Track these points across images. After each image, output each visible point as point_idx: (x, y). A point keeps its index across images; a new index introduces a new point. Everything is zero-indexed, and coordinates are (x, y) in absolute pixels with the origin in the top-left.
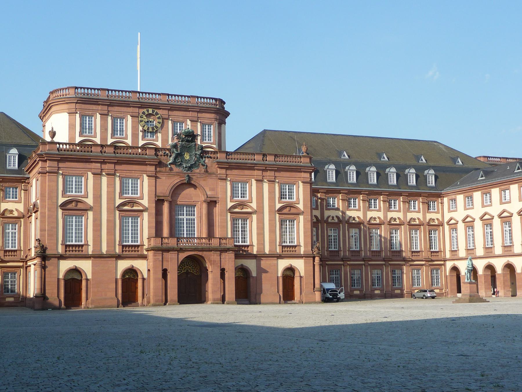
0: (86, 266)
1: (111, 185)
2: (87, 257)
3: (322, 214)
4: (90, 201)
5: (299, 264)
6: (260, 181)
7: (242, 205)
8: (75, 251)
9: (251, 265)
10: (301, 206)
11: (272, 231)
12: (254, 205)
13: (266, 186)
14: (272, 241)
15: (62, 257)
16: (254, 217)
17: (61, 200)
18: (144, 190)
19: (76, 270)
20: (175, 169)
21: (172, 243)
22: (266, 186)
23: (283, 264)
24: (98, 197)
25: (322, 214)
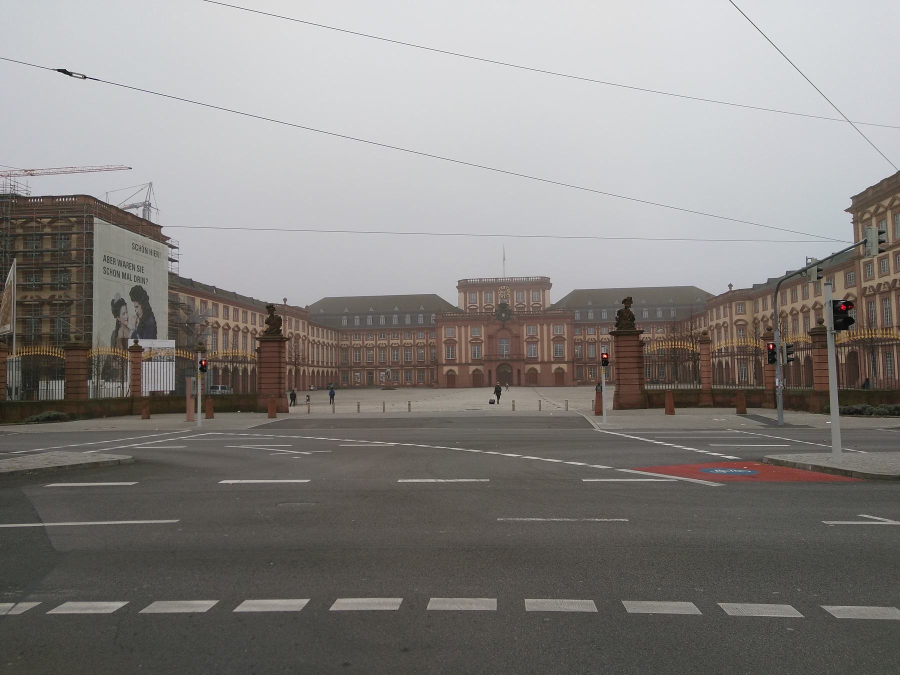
0: (456, 369)
1: (466, 332)
2: (457, 365)
3: (598, 337)
4: (457, 339)
5: (564, 367)
6: (542, 325)
7: (532, 337)
8: (451, 362)
9: (538, 367)
10: (565, 337)
11: (549, 350)
12: (539, 337)
13: (545, 327)
14: (549, 355)
15: (445, 365)
16: (539, 343)
17: (444, 339)
18: (482, 332)
19: (451, 370)
20: (497, 322)
21: (493, 358)
22: (545, 327)
23: (554, 367)
24: (460, 337)
25: (598, 337)
